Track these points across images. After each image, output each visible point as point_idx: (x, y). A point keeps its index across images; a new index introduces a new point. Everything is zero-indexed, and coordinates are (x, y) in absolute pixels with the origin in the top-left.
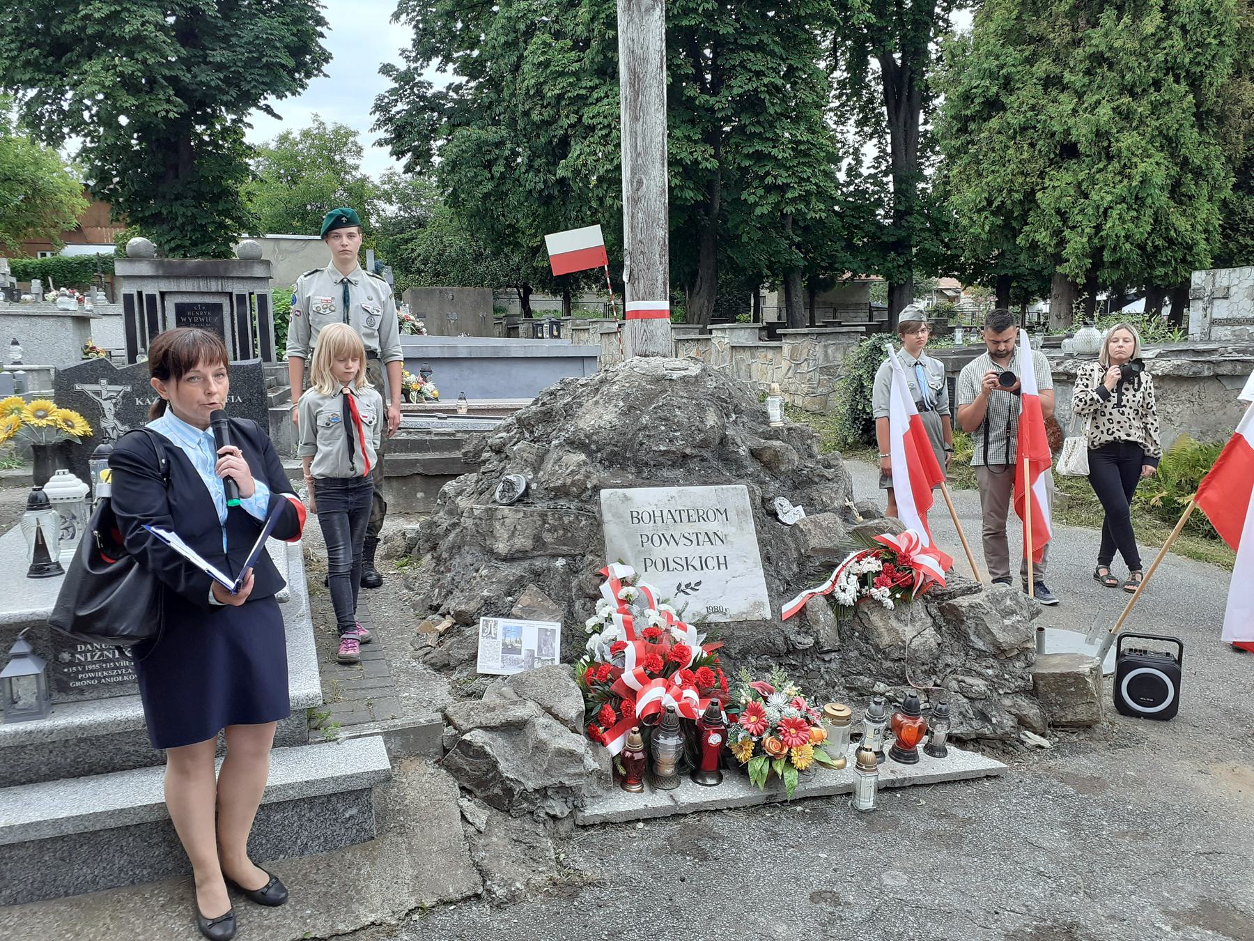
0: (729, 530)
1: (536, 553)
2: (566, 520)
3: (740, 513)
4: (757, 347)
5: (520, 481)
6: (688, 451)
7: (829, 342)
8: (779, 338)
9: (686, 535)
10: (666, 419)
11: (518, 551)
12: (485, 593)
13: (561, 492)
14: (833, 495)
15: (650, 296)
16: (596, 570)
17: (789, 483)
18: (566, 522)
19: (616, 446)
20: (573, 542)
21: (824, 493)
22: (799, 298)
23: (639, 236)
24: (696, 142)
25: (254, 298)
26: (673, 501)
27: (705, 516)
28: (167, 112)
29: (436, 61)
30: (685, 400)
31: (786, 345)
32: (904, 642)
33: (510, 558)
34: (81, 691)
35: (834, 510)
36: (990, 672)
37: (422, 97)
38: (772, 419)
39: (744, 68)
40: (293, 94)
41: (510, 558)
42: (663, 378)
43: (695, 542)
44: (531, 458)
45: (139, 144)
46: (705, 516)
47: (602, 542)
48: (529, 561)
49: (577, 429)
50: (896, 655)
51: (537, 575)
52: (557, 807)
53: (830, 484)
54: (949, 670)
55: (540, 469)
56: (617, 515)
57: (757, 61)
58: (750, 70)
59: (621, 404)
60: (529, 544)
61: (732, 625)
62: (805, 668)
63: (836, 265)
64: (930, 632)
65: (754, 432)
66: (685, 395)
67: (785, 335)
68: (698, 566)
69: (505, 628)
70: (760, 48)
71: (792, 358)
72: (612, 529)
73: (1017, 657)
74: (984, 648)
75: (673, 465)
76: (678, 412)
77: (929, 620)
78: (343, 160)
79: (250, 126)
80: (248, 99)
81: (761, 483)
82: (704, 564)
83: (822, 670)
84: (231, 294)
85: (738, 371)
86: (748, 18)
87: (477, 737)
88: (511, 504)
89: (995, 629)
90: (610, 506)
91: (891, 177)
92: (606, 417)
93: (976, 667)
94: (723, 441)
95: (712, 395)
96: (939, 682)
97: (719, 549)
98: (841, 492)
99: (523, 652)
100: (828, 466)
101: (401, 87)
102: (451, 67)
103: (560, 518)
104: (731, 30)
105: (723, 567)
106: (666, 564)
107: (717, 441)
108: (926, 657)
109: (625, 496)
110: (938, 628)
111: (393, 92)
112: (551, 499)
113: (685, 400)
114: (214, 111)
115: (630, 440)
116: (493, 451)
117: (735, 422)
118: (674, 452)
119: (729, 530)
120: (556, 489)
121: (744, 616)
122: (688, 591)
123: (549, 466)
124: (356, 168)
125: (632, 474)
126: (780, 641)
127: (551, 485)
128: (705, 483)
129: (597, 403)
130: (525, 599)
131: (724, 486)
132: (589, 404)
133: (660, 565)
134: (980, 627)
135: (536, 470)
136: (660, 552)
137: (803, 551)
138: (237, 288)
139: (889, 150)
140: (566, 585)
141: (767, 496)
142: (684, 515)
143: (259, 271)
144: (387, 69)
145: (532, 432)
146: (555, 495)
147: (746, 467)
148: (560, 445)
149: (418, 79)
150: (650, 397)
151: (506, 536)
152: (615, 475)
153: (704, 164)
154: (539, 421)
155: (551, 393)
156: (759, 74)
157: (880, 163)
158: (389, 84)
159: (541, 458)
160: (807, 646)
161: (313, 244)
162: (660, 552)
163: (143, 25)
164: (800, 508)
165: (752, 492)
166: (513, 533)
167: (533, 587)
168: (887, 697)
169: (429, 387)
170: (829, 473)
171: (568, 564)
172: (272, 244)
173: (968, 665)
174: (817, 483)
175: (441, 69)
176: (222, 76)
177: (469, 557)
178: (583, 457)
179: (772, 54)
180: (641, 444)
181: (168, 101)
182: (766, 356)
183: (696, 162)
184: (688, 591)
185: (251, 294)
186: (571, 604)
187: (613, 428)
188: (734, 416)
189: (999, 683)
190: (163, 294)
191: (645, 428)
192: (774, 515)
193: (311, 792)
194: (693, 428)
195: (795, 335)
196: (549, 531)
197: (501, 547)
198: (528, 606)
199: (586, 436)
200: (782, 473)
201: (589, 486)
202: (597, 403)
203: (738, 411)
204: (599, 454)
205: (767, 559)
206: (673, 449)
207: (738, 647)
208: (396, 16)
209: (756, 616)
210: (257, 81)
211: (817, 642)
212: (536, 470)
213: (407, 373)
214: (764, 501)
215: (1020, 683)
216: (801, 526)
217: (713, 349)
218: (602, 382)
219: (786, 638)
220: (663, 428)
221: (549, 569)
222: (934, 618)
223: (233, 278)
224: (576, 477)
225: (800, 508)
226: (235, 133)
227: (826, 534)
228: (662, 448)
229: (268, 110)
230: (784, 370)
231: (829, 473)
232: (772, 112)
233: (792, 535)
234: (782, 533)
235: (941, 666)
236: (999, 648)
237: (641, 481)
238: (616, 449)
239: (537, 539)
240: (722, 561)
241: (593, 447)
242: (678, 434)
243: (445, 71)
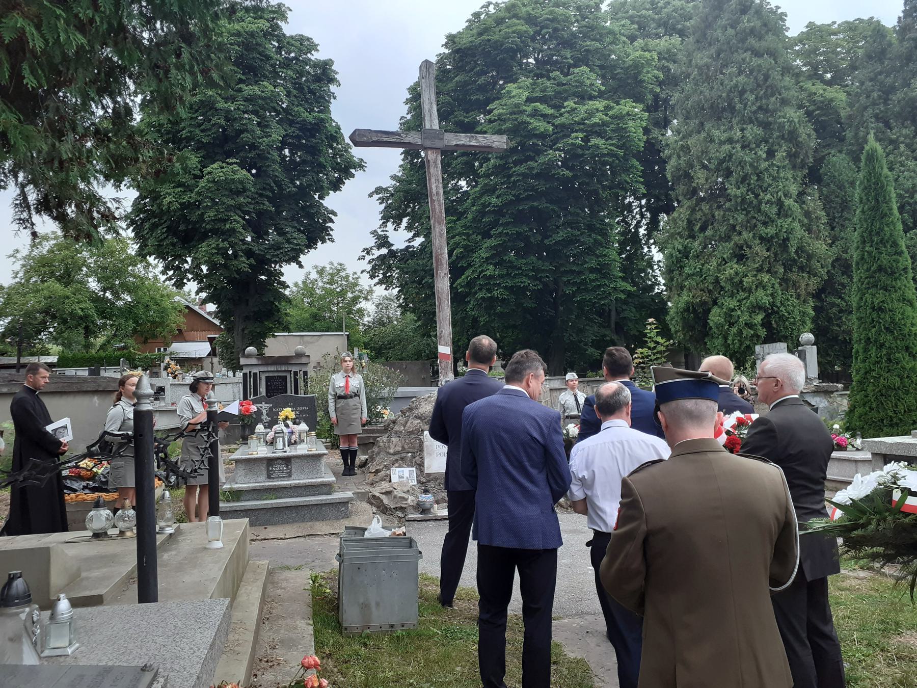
13: (411, 433)
20: (414, 448)
33: (394, 454)
34: (273, 478)
41: (394, 454)
44: (403, 422)
51: (402, 459)
52: (400, 514)
87: (378, 495)
123: (408, 424)
135: (404, 427)
143: (304, 360)
154: (407, 411)
159: (406, 423)
161: (324, 337)
172: (298, 338)
193: (333, 502)
197: (391, 451)
212: (404, 427)
239: (403, 447)
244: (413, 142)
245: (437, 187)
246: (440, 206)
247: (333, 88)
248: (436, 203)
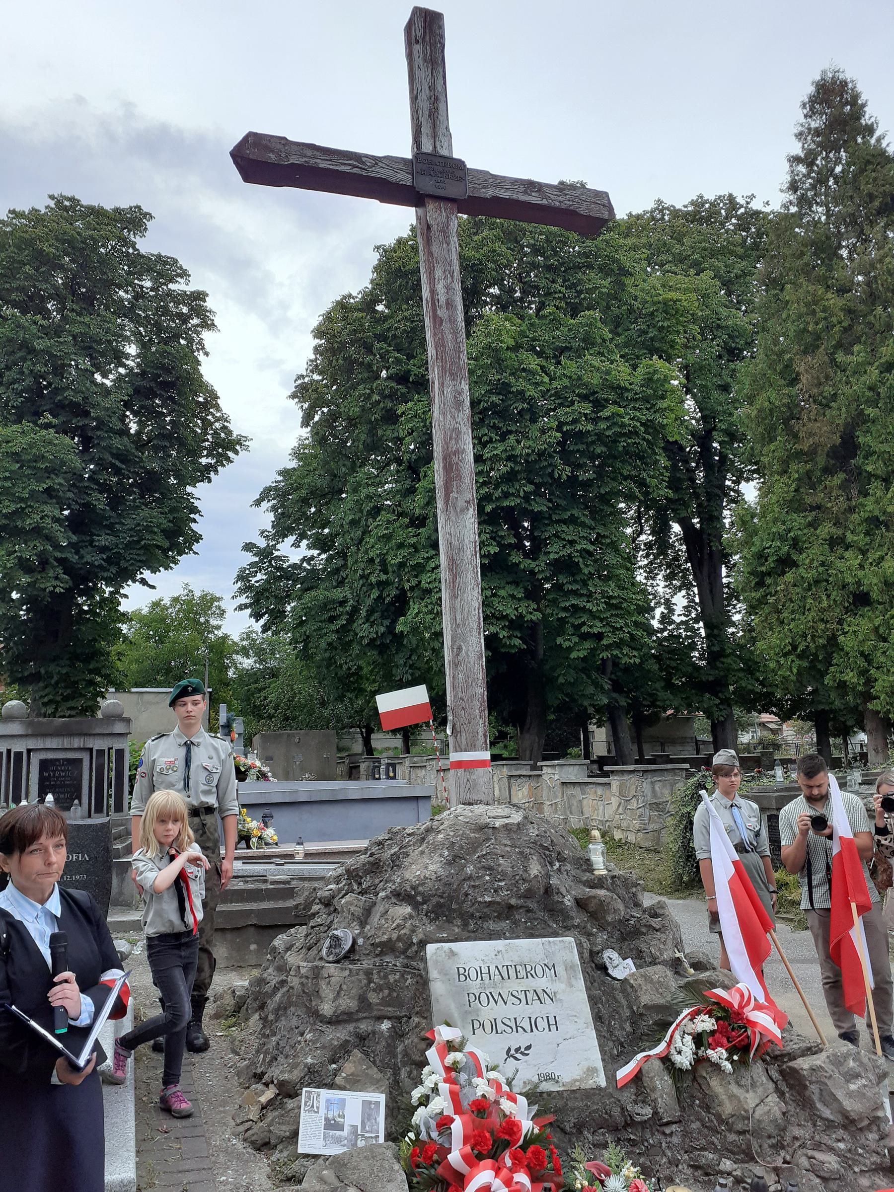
0: (558, 987)
1: (361, 1015)
2: (392, 978)
3: (569, 968)
4: (587, 784)
5: (346, 934)
6: (513, 901)
7: (656, 779)
8: (606, 774)
9: (515, 993)
10: (490, 868)
11: (343, 1013)
12: (309, 1060)
13: (387, 947)
14: (662, 946)
15: (471, 747)
16: (423, 1033)
17: (617, 934)
18: (392, 981)
19: (442, 897)
20: (399, 1004)
21: (653, 945)
22: (626, 735)
23: (460, 695)
24: (519, 599)
25: (113, 752)
26: (500, 956)
27: (533, 972)
28: (55, 587)
29: (291, 539)
30: (508, 849)
31: (615, 781)
32: (746, 1111)
33: (335, 1021)
35: (664, 963)
36: (842, 1145)
37: (279, 569)
38: (595, 867)
39: (559, 537)
40: (166, 569)
41: (335, 1021)
42: (487, 826)
43: (524, 1001)
44: (358, 911)
45: (28, 614)
46: (533, 972)
47: (428, 1002)
48: (354, 1025)
49: (404, 881)
50: (739, 1126)
51: (362, 1039)
53: (658, 935)
54: (797, 1144)
55: (366, 923)
56: (443, 972)
57: (569, 532)
58: (564, 539)
59: (446, 853)
60: (353, 1005)
61: (565, 1094)
62: (646, 1144)
63: (658, 703)
64: (773, 1099)
65: (577, 880)
66: (509, 843)
67: (612, 772)
68: (528, 1028)
69: (327, 1101)
70: (572, 521)
71: (621, 794)
72: (438, 988)
73: (868, 1128)
74: (832, 1118)
75: (499, 917)
76: (501, 861)
77: (771, 1086)
78: (207, 621)
79: (126, 596)
80: (126, 574)
81: (589, 935)
83: (664, 1145)
84: (91, 750)
85: (570, 807)
86: (560, 497)
88: (337, 962)
89: (840, 1095)
90: (437, 961)
91: (701, 624)
92: (431, 868)
93: (825, 1139)
94: (548, 890)
95: (535, 843)
96: (788, 1158)
97: (549, 1009)
98: (670, 943)
99: (346, 1128)
100: (655, 915)
101: (261, 561)
102: (304, 543)
103: (386, 977)
104: (545, 509)
105: (553, 1028)
107: (542, 891)
108: (771, 1129)
109: (451, 951)
110: (781, 1094)
111: (252, 565)
112: (377, 955)
113: (508, 849)
114: (95, 585)
115: (455, 891)
116: (321, 902)
117: (559, 870)
118: (499, 903)
119: (558, 987)
120: (381, 944)
121: (577, 1084)
122: (518, 1056)
123: (375, 919)
124: (219, 627)
125: (459, 927)
126: (616, 1112)
127: (377, 940)
128: (532, 936)
129: (422, 852)
130: (349, 1067)
131: (551, 939)
132: (415, 854)
134: (824, 1093)
135: (363, 924)
136: (488, 1012)
137: (635, 1008)
138: (98, 744)
139: (697, 600)
140: (391, 1051)
141: (595, 949)
143: (119, 728)
144: (248, 547)
145: (360, 884)
146: (381, 952)
147: (572, 918)
148: (387, 897)
149: (276, 553)
150: (474, 846)
151: (331, 996)
152: (440, 929)
153: (528, 617)
154: (367, 872)
155: (380, 843)
156: (572, 543)
157: (690, 612)
158: (250, 558)
159: (368, 911)
160: (645, 1118)
162: (488, 1012)
163: (41, 519)
164: (629, 961)
165: (579, 945)
166: (338, 993)
167: (357, 1053)
168: (735, 1177)
169: (270, 833)
170: (656, 923)
171: (393, 1027)
172: (136, 696)
173: (817, 1138)
174: (644, 934)
175: (296, 545)
176: (105, 557)
177: (295, 1018)
178: (408, 910)
179: (583, 525)
180: (466, 895)
181: (56, 578)
182: (596, 792)
183: (521, 616)
184: (518, 1056)
185: (110, 749)
186: (396, 1072)
187: (439, 879)
188: (557, 864)
189: (853, 1160)
190: (29, 751)
191: (470, 878)
192: (604, 968)
194: (517, 877)
195: (623, 772)
196: (374, 990)
197: (327, 1009)
198: (352, 1074)
199: (413, 888)
200: (609, 924)
201: (415, 941)
202: (422, 852)
203: (561, 859)
204: (425, 907)
205: (598, 1018)
206: (498, 899)
207: (573, 1120)
208: (258, 503)
209: (590, 1084)
210: (135, 560)
211: (655, 1113)
212: (363, 924)
213: (249, 819)
215: (875, 1158)
216: (632, 982)
217: (544, 785)
218: (428, 830)
219: (623, 1109)
220: (487, 878)
221: (374, 1033)
222: (775, 1083)
223: (94, 735)
224: (402, 932)
225: (629, 961)
226: (112, 602)
227: (657, 989)
228: (488, 899)
229: (144, 582)
230: (615, 806)
231: (656, 923)
232: (587, 572)
233: (623, 991)
234: (613, 989)
235: (788, 1139)
236: (847, 1118)
237: (468, 934)
238: (442, 900)
239: (363, 999)
240: (552, 1021)
241: (419, 899)
242: (502, 884)
243: (299, 546)
244: (393, 180)
245: (448, 288)
246: (455, 333)
247: (207, 336)
248: (446, 326)
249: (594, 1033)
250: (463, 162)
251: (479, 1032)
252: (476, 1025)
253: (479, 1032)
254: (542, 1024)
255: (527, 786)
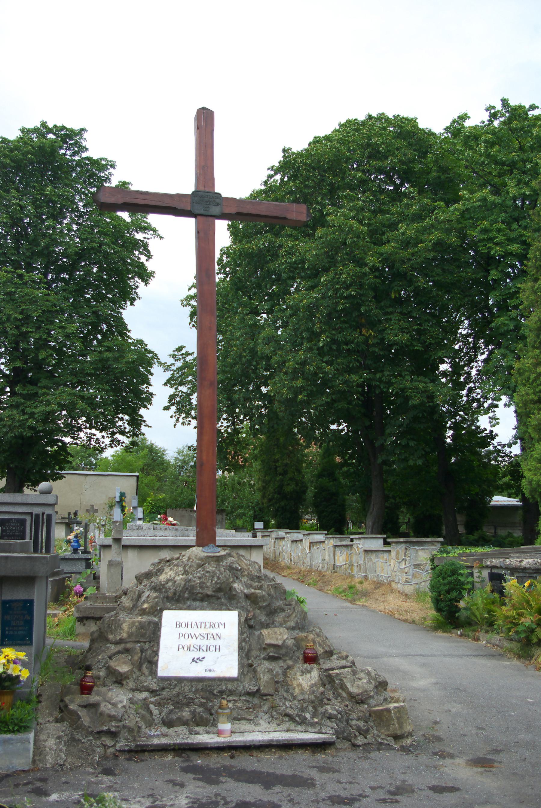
25: (45, 517)
68: (205, 649)
82: (208, 649)
89: (349, 685)
97: (218, 642)
105: (217, 650)
106: (189, 648)
133: (186, 648)
142: (203, 625)
165: (240, 616)
172: (83, 478)
185: (43, 514)
205: (241, 648)
214: (246, 620)
215: (361, 714)
240: (218, 647)
249: (237, 654)
250: (220, 194)
251: (181, 650)
252: (181, 647)
253: (181, 650)
254: (212, 648)
255: (345, 553)
